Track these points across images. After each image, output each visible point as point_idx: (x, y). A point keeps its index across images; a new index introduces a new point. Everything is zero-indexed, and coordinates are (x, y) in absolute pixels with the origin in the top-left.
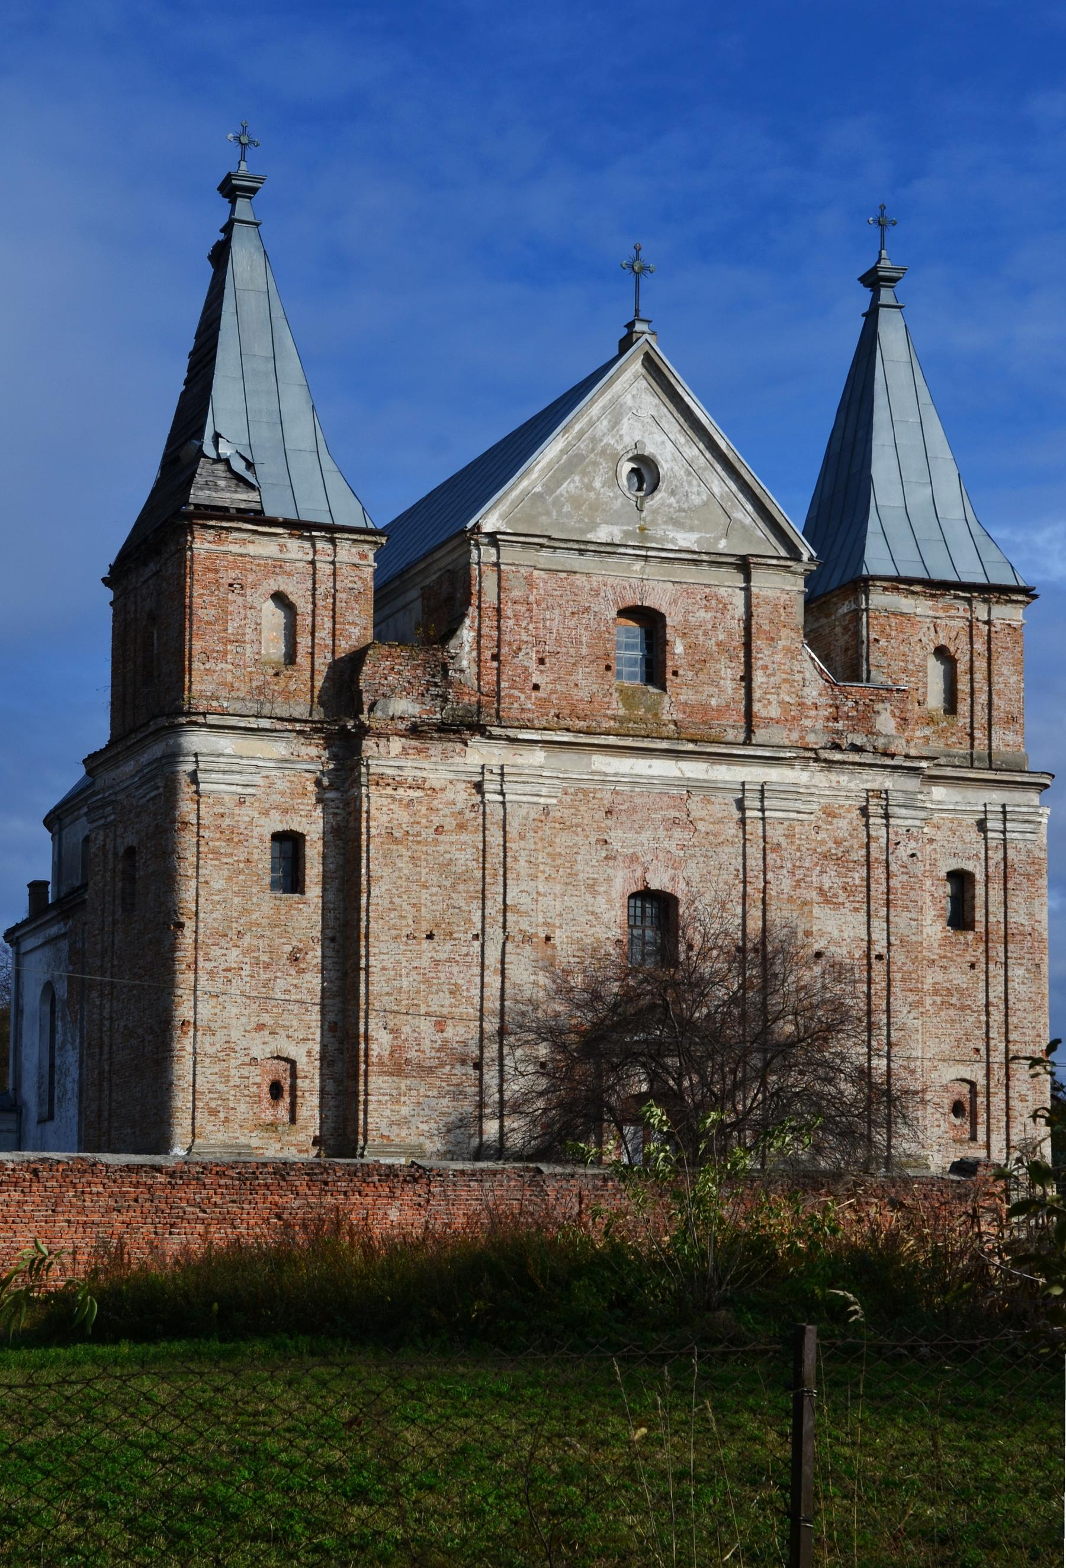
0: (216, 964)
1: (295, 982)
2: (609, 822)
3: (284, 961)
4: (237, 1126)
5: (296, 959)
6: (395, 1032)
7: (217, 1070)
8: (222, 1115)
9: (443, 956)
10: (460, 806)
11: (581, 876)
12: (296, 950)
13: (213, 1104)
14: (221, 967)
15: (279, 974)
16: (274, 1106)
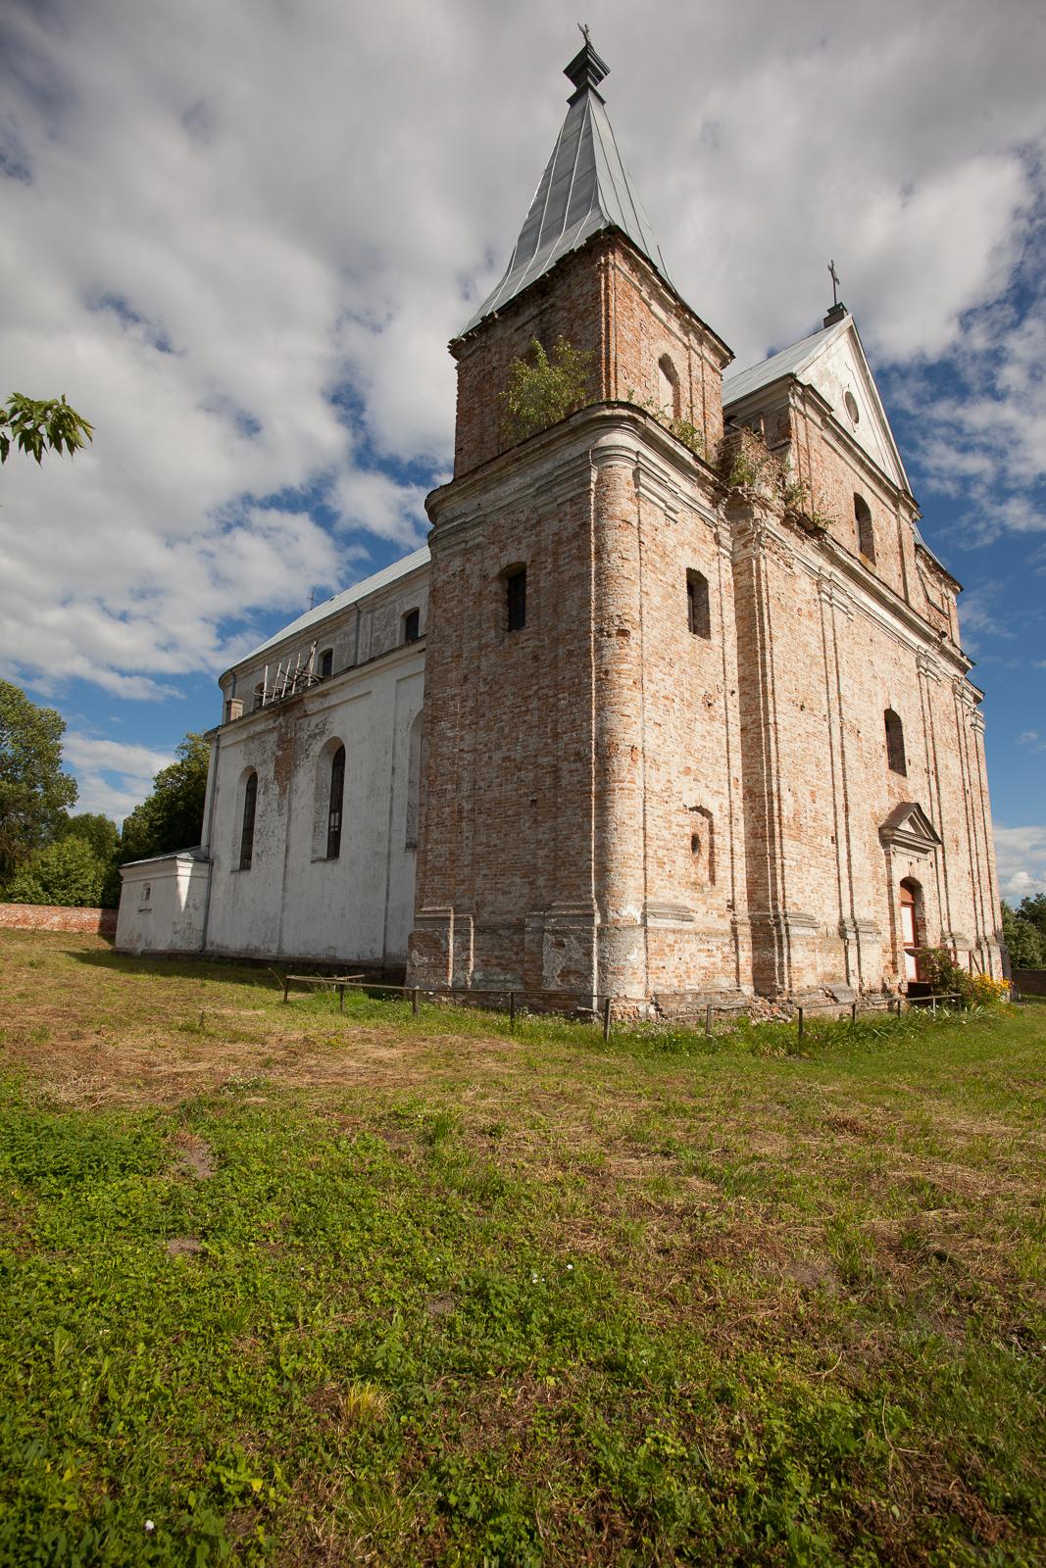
0: (657, 688)
1: (709, 728)
2: (871, 648)
3: (699, 703)
4: (676, 883)
5: (710, 705)
6: (794, 794)
7: (661, 813)
8: (667, 867)
9: (810, 730)
10: (808, 597)
11: (866, 686)
12: (707, 696)
13: (661, 853)
14: (663, 693)
15: (698, 717)
16: (696, 862)
